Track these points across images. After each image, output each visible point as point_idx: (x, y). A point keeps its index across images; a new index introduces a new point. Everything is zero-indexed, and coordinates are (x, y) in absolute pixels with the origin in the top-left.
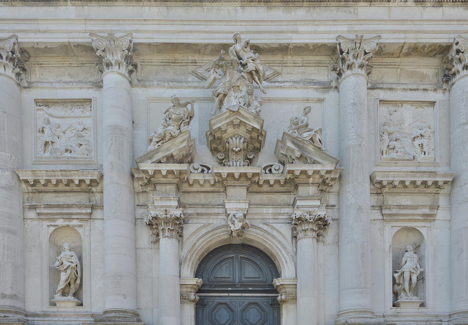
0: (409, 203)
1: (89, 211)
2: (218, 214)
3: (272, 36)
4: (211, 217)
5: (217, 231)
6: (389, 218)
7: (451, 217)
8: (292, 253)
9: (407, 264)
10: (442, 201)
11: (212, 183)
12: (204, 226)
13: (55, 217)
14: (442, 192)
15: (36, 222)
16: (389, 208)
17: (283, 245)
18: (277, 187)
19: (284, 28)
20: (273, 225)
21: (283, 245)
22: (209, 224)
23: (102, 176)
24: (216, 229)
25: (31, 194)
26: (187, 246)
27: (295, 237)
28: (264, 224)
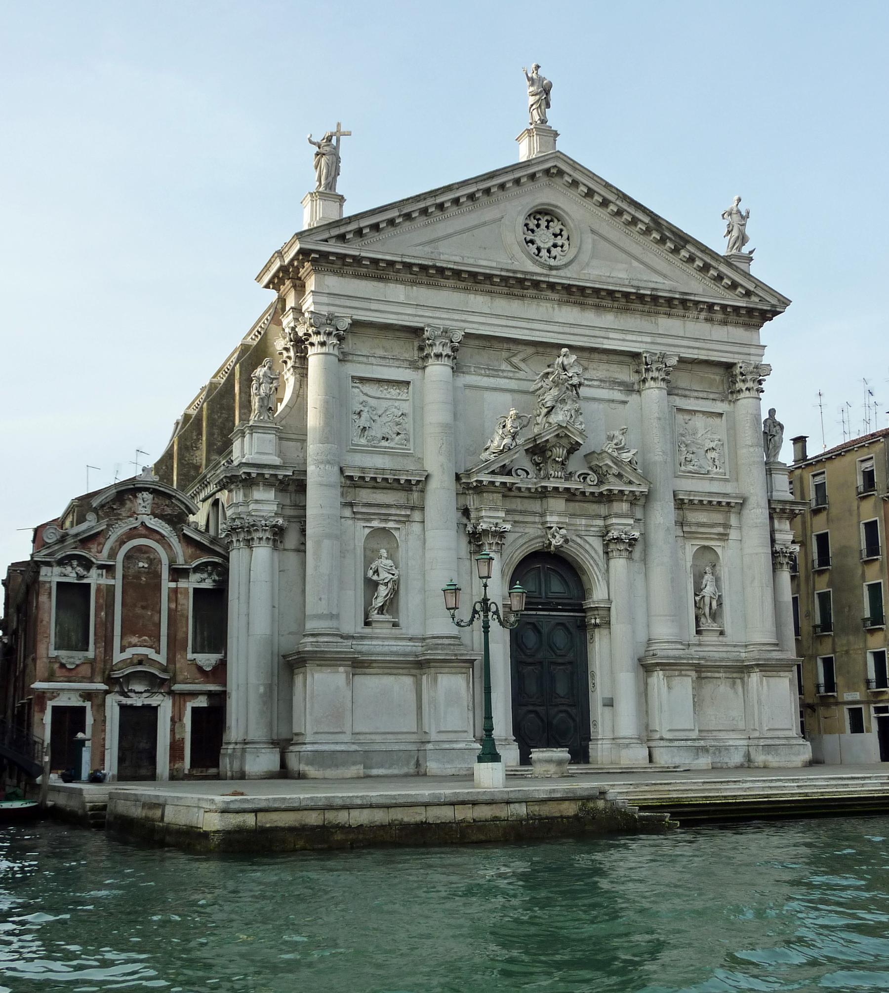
0: (705, 520)
1: (408, 513)
2: (535, 523)
3: (586, 339)
4: (528, 525)
5: (533, 542)
6: (689, 535)
7: (742, 537)
8: (603, 570)
9: (708, 587)
10: (733, 520)
11: (533, 490)
12: (521, 536)
13: (372, 517)
14: (733, 510)
15: (350, 522)
16: (690, 525)
17: (595, 561)
18: (591, 498)
19: (598, 333)
20: (586, 538)
21: (595, 561)
22: (526, 533)
23: (427, 477)
24: (532, 539)
25: (345, 489)
26: (505, 556)
27: (607, 553)
28: (578, 536)
